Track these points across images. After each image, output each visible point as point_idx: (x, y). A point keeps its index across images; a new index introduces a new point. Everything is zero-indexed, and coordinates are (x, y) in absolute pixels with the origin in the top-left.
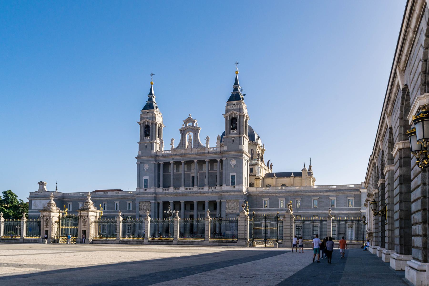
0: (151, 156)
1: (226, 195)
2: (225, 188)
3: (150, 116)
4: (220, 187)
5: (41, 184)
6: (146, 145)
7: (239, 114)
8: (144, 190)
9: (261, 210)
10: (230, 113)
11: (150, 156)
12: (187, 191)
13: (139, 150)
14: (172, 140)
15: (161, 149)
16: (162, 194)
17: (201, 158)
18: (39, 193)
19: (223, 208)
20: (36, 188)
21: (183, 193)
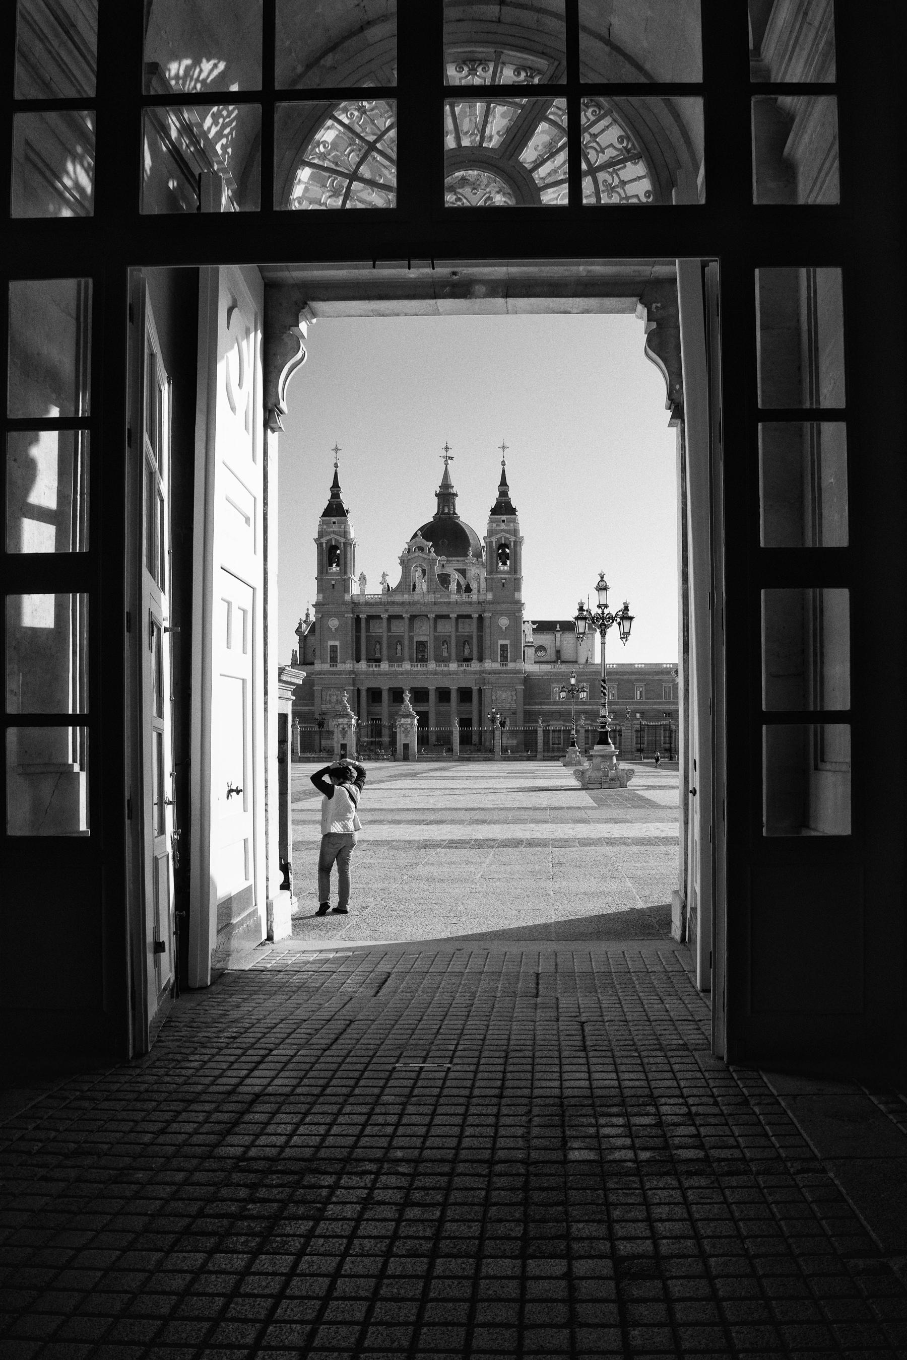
0: (345, 603)
1: (492, 678)
2: (489, 665)
6: (333, 582)
8: (331, 666)
9: (548, 704)
10: (498, 536)
13: (318, 592)
14: (384, 575)
15: (363, 591)
16: (366, 673)
17: (444, 610)
19: (486, 700)
21: (408, 673)
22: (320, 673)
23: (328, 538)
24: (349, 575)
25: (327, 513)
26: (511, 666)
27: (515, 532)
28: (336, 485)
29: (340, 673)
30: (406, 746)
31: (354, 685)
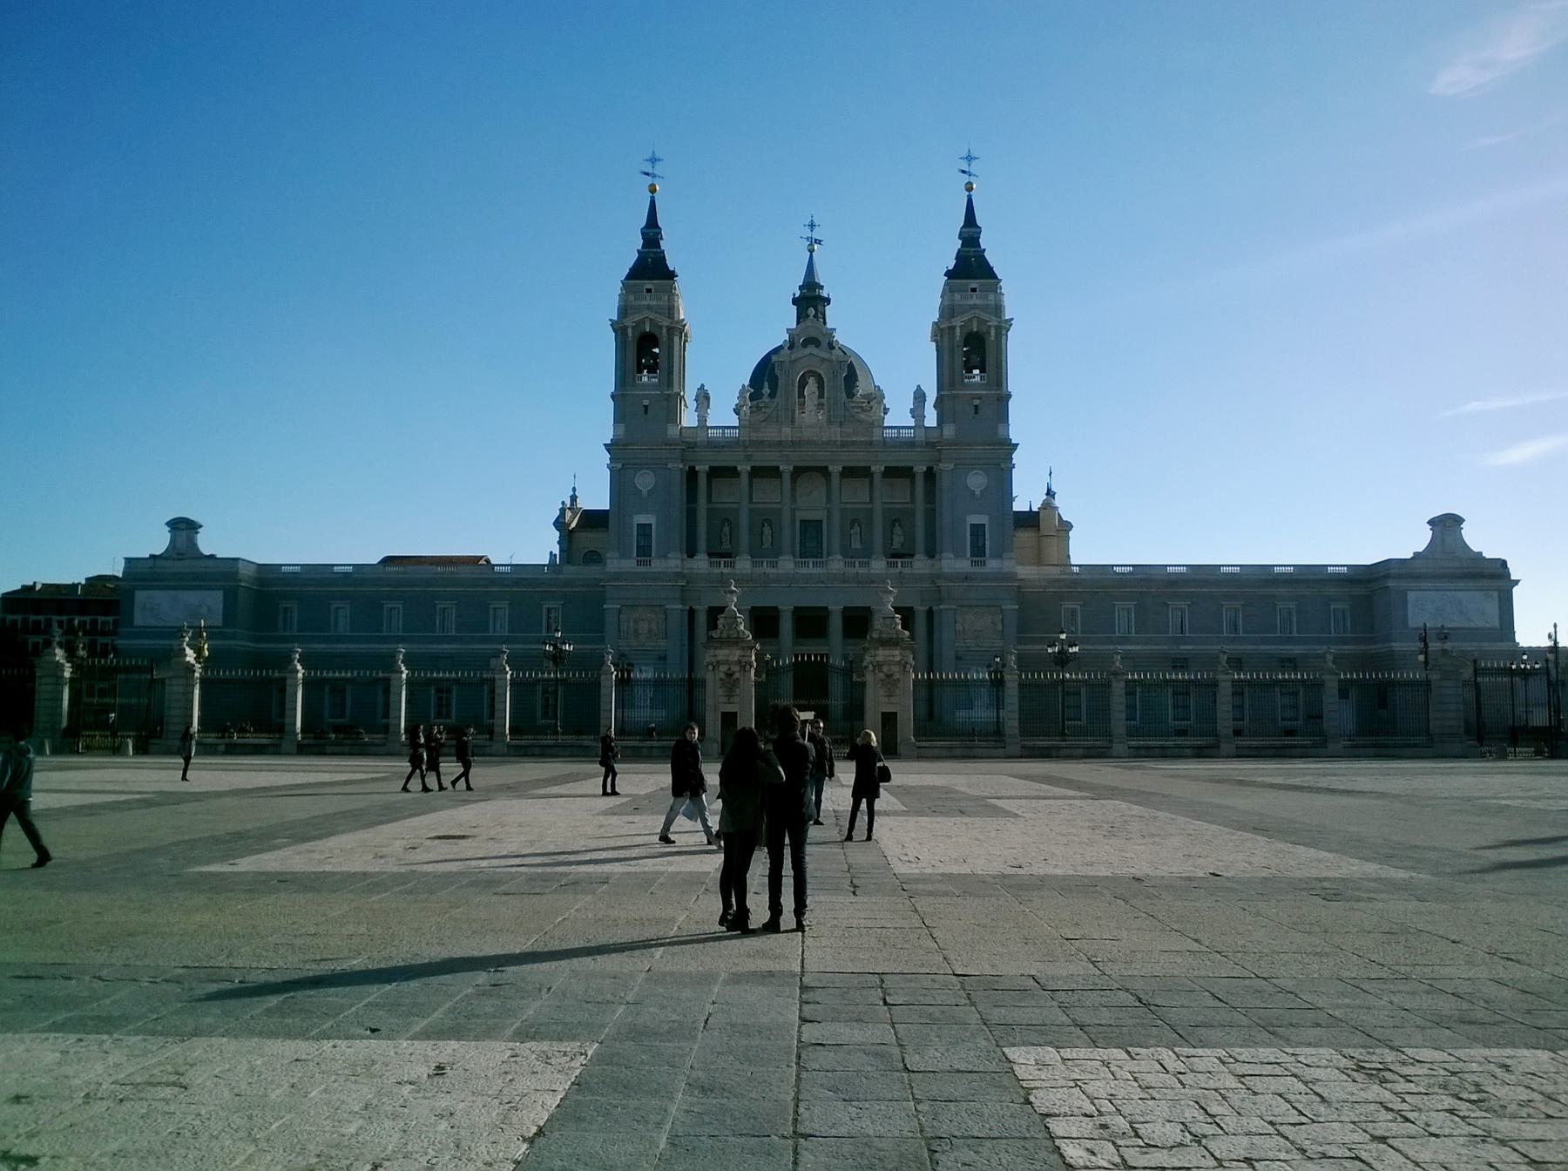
2: (954, 564)
3: (661, 303)
4: (930, 561)
5: (184, 526)
6: (646, 402)
7: (996, 323)
8: (639, 563)
11: (666, 445)
12: (804, 570)
15: (702, 419)
17: (858, 459)
18: (169, 563)
20: (157, 542)
22: (618, 576)
23: (637, 317)
24: (676, 389)
25: (637, 272)
26: (992, 565)
27: (998, 309)
28: (652, 224)
29: (657, 577)
30: (889, 720)
31: (683, 602)
